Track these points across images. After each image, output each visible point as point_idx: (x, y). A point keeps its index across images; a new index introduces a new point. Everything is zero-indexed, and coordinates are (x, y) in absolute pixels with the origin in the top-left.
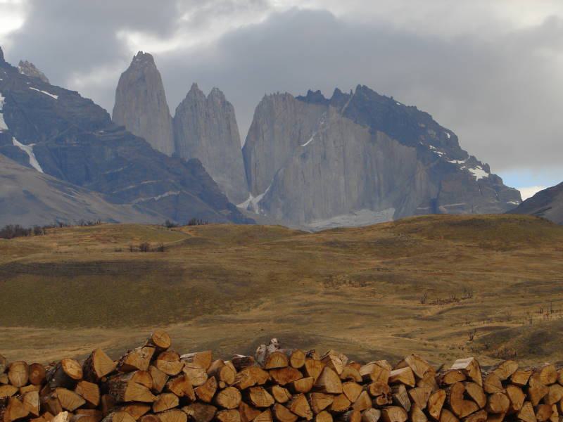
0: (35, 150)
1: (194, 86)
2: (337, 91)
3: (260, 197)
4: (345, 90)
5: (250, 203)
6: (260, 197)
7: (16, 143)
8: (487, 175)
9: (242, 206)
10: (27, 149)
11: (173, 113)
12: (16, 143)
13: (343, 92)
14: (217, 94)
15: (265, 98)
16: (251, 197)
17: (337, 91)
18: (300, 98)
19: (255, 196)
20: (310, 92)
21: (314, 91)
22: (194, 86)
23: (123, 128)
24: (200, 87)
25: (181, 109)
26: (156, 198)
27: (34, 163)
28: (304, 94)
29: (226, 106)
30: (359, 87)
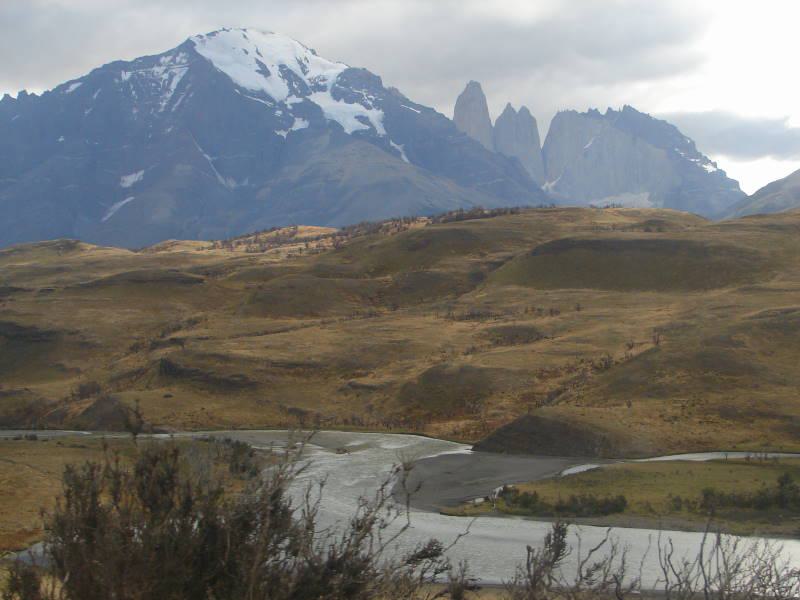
1: (509, 104)
3: (553, 184)
4: (616, 108)
5: (547, 186)
6: (553, 184)
7: (392, 144)
8: (715, 169)
9: (544, 188)
10: (399, 148)
11: (493, 124)
12: (392, 144)
13: (614, 109)
14: (524, 111)
15: (558, 113)
16: (547, 184)
18: (583, 114)
19: (550, 182)
20: (590, 110)
21: (593, 108)
22: (509, 104)
23: (465, 134)
24: (513, 106)
25: (499, 120)
27: (404, 157)
28: (586, 111)
29: (532, 121)
30: (625, 106)
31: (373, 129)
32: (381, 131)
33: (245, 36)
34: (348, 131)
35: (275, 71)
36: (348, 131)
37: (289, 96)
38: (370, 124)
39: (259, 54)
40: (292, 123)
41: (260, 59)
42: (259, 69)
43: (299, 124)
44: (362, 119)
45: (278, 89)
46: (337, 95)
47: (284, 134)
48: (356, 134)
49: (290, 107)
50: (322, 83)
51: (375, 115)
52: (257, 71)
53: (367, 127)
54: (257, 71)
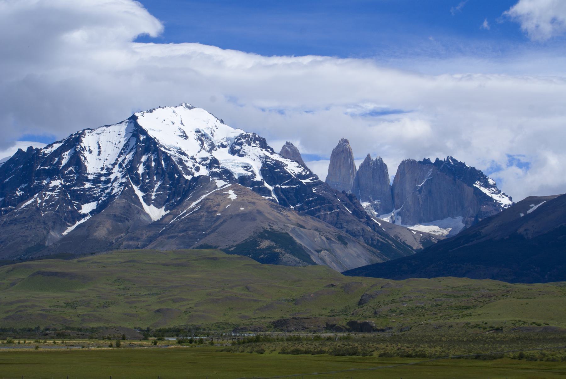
0: (276, 190)
2: (437, 160)
10: (271, 188)
12: (266, 185)
17: (437, 160)
18: (420, 162)
20: (424, 159)
26: (329, 213)
28: (422, 160)
31: (254, 175)
32: (259, 178)
33: (174, 112)
35: (192, 136)
37: (199, 152)
38: (252, 171)
39: (182, 124)
40: (198, 169)
41: (182, 127)
42: (181, 134)
44: (247, 167)
45: (191, 147)
46: (233, 152)
47: (189, 178)
49: (198, 160)
50: (225, 143)
51: (257, 166)
52: (179, 136)
53: (250, 174)
54: (179, 136)
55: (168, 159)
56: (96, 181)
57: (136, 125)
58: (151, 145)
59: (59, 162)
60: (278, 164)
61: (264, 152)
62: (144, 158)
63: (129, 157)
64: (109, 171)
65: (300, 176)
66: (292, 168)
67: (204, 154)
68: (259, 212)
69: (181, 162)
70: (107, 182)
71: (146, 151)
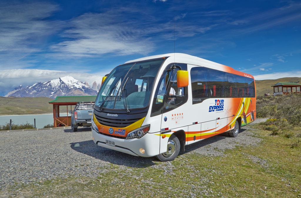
32: (81, 88)
34: (77, 88)
36: (77, 88)
43: (72, 87)
45: (70, 83)
46: (77, 84)
48: (78, 88)
51: (81, 87)
55: (66, 85)
56: (54, 88)
57: (60, 79)
58: (63, 83)
59: (47, 85)
60: (84, 86)
61: (82, 84)
62: (62, 85)
63: (59, 85)
64: (56, 87)
65: (88, 88)
66: (86, 86)
67: (72, 84)
68: (82, 94)
69: (68, 86)
70: (56, 89)
71: (62, 83)
